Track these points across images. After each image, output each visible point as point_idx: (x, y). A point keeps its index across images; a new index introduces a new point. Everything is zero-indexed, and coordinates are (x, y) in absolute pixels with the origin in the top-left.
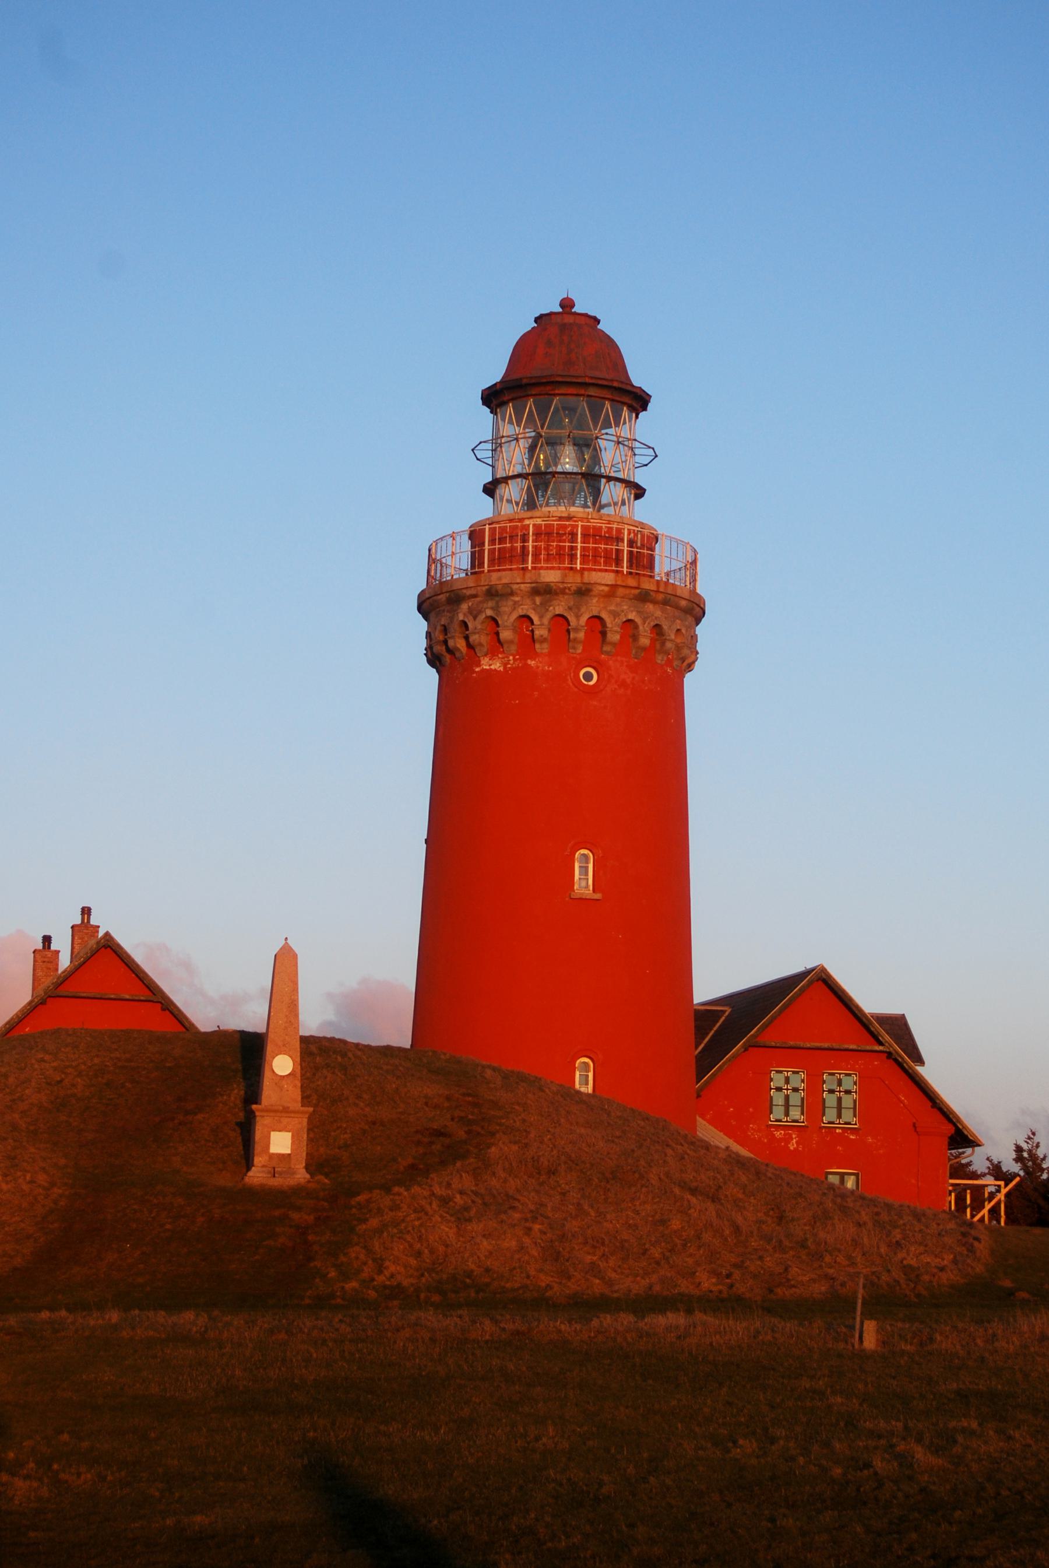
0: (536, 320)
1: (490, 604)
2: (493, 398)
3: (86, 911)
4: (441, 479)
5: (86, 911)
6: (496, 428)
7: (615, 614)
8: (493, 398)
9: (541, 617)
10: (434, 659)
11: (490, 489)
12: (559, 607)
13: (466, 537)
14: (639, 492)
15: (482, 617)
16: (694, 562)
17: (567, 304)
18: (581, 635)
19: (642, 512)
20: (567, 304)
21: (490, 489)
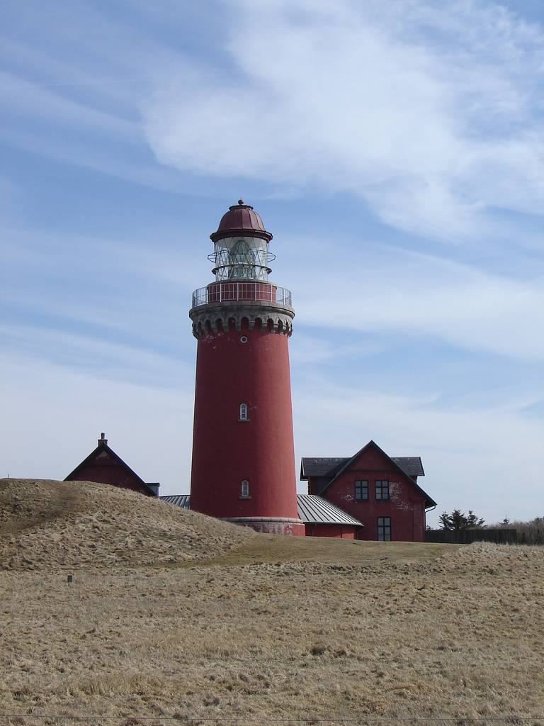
0: (230, 208)
1: (208, 315)
2: (215, 238)
3: (103, 435)
4: (196, 270)
5: (103, 435)
6: (216, 249)
7: (252, 316)
8: (215, 238)
9: (225, 319)
10: (196, 334)
11: (214, 271)
12: (231, 315)
13: (205, 289)
14: (269, 271)
15: (205, 320)
16: (290, 296)
17: (240, 202)
18: (240, 324)
19: (271, 279)
20: (240, 202)
21: (214, 271)
